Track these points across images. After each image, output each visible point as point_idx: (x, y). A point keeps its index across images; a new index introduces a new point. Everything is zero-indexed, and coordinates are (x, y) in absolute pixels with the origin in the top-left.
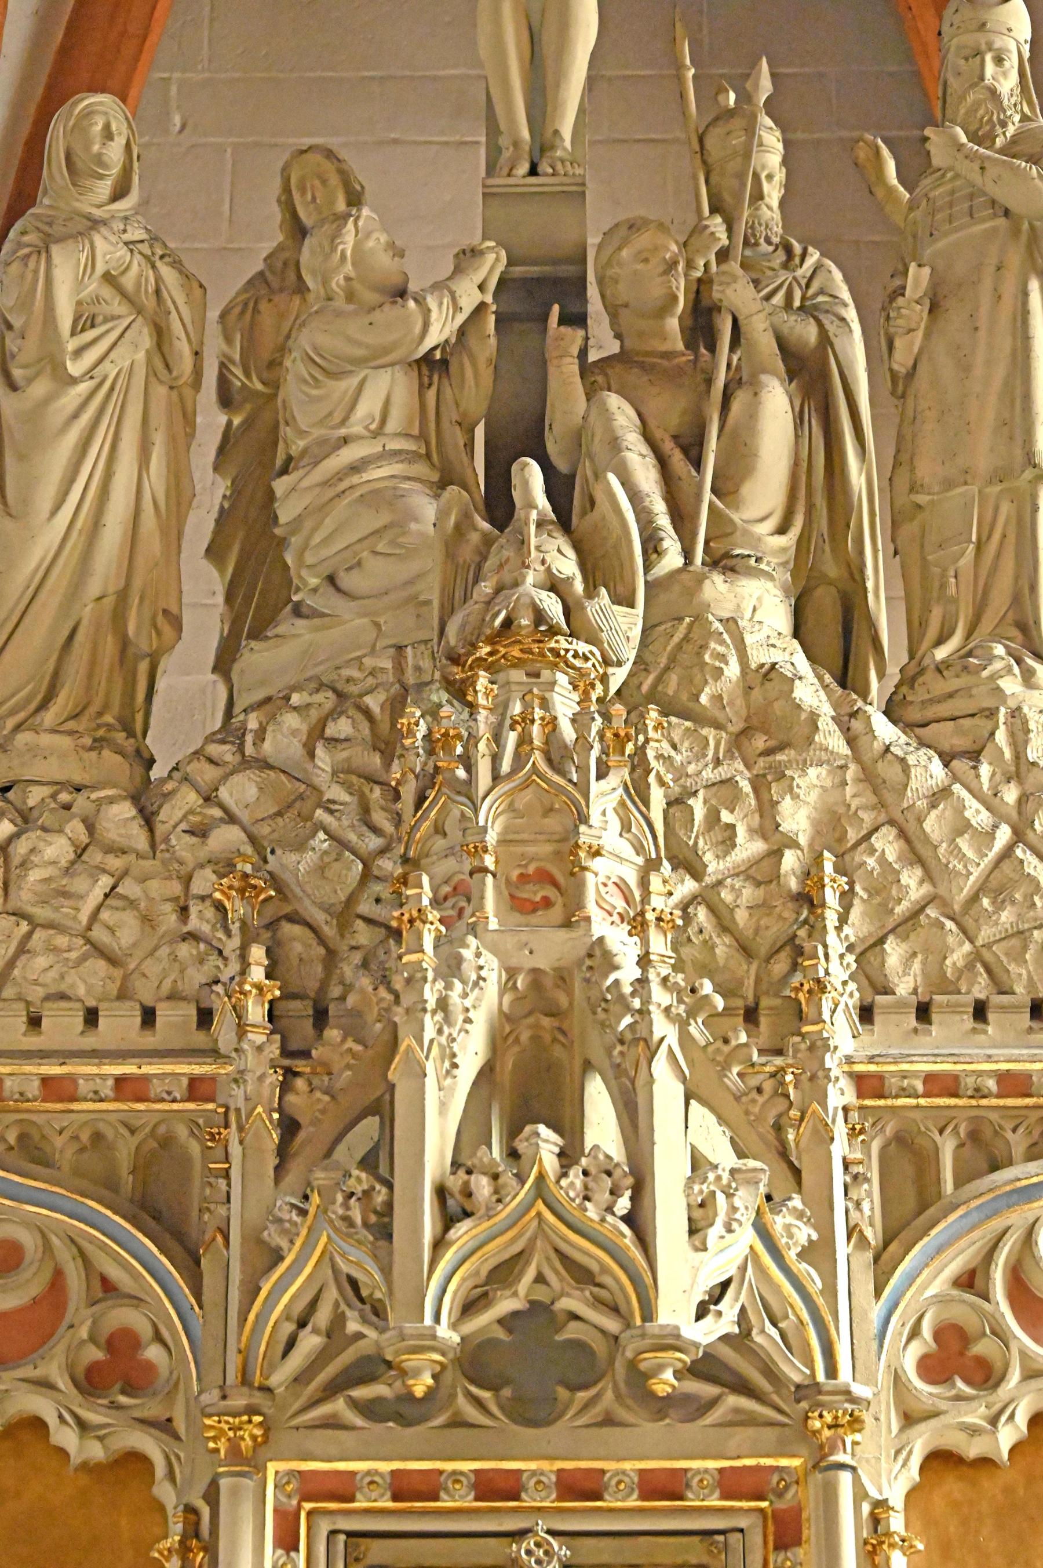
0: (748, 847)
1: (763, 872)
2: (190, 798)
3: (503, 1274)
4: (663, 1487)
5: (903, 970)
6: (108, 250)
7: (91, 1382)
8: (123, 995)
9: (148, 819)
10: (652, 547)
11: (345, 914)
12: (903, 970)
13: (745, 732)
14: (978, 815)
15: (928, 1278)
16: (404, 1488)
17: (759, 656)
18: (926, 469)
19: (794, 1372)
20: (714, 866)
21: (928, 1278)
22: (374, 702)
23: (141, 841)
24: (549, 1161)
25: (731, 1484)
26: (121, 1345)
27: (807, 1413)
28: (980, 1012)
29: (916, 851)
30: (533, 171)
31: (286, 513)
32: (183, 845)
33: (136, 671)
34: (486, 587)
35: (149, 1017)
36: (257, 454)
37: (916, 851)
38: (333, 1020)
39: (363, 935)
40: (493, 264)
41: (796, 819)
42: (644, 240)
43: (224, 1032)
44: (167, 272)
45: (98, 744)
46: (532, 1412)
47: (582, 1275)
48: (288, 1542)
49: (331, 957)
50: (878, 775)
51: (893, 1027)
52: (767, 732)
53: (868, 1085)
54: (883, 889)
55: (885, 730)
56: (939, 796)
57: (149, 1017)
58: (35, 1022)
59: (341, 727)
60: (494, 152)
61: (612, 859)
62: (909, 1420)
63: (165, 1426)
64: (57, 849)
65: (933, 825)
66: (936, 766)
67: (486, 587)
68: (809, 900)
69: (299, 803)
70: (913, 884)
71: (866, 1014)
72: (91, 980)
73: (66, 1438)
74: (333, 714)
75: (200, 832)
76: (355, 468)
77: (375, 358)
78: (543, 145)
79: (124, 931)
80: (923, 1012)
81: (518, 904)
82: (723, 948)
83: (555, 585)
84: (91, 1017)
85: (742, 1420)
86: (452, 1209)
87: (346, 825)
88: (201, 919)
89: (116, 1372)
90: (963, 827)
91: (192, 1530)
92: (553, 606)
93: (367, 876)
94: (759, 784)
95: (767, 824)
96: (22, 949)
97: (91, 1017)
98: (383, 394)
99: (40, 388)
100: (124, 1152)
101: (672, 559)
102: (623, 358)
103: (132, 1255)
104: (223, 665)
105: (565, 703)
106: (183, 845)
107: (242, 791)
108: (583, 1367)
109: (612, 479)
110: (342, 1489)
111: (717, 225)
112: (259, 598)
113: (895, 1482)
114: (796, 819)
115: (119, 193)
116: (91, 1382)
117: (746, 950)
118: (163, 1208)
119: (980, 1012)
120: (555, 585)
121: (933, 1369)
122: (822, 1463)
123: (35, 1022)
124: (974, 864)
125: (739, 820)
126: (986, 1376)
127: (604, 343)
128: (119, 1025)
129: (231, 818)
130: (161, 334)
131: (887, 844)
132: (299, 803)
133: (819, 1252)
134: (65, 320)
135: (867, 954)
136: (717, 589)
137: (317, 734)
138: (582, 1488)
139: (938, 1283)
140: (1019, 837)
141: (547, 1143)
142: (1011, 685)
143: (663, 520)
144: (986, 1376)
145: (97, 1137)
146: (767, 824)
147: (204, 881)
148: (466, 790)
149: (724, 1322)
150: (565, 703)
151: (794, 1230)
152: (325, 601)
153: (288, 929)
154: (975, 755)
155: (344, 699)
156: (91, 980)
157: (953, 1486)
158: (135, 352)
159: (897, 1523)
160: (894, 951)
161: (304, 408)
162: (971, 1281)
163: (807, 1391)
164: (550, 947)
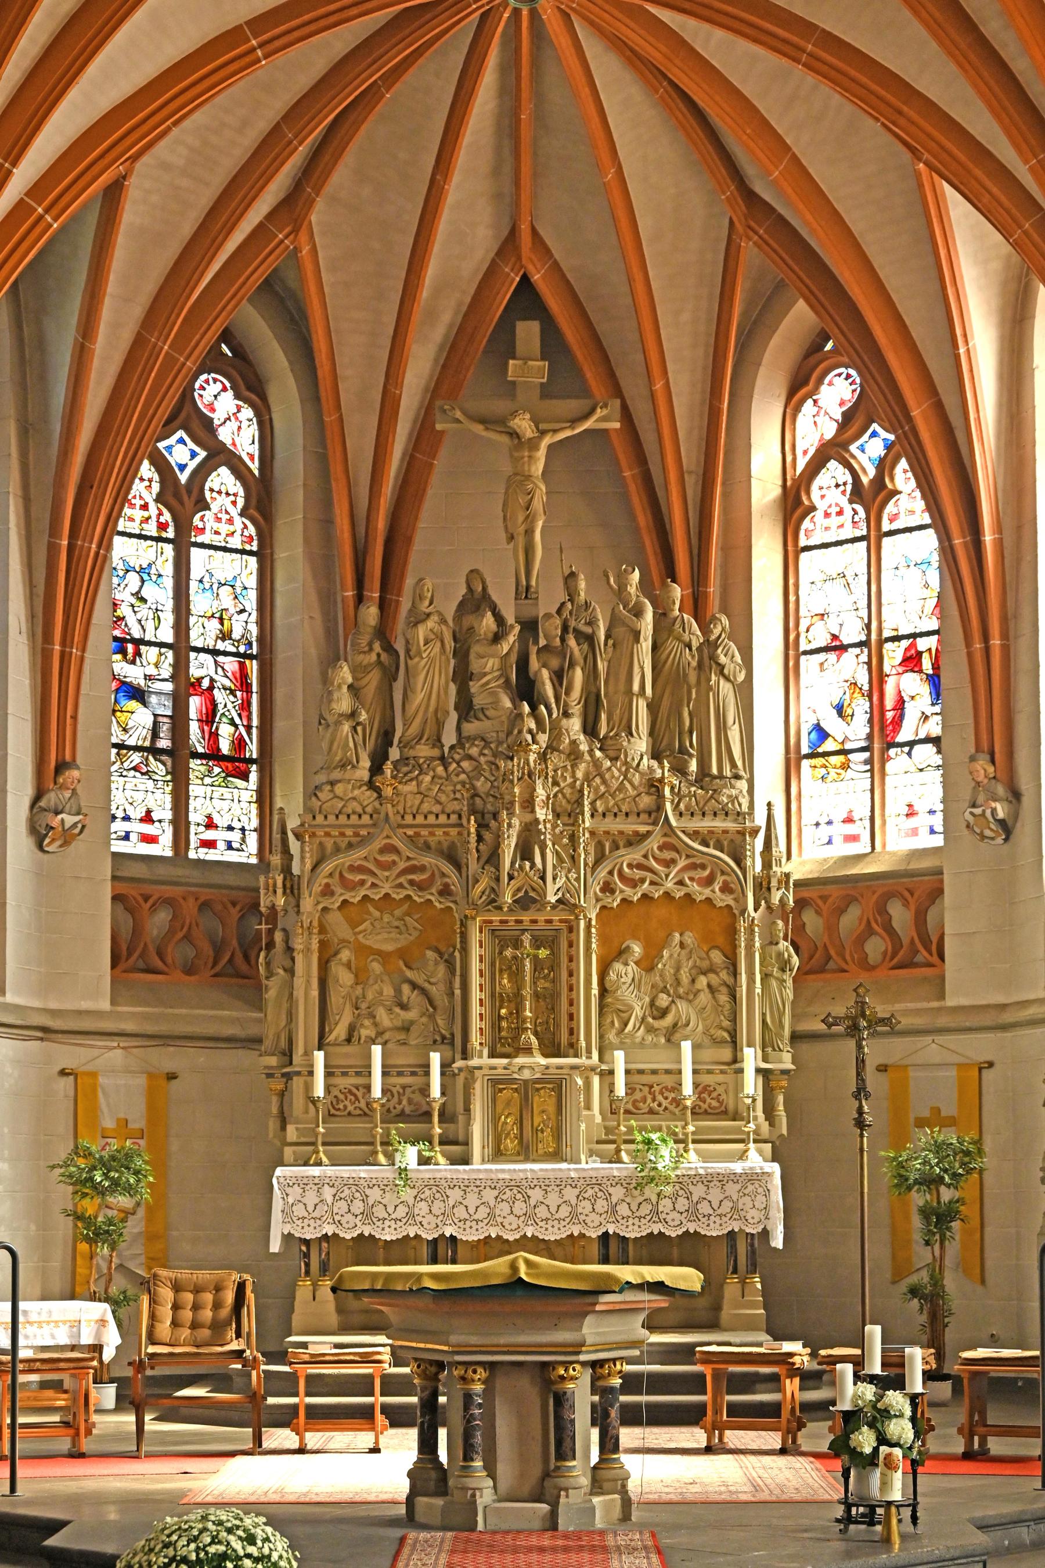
0: (569, 780)
1: (572, 785)
2: (454, 765)
3: (519, 890)
4: (550, 921)
5: (600, 806)
6: (430, 624)
7: (441, 893)
8: (443, 812)
9: (446, 769)
10: (550, 714)
11: (488, 794)
12: (600, 806)
13: (569, 755)
14: (616, 773)
15: (602, 873)
16: (501, 922)
17: (573, 738)
18: (611, 688)
19: (572, 901)
20: (562, 785)
21: (602, 873)
22: (493, 746)
23: (444, 775)
24: (528, 868)
25: (561, 921)
26: (446, 886)
27: (574, 908)
28: (615, 815)
29: (604, 782)
30: (526, 597)
31: (473, 690)
32: (455, 779)
33: (440, 725)
34: (516, 732)
35: (449, 816)
36: (462, 655)
37: (604, 782)
38: (487, 821)
39: (491, 799)
40: (518, 628)
41: (580, 774)
42: (551, 621)
43: (464, 821)
44: (444, 628)
45: (434, 746)
46: (525, 908)
47: (534, 890)
48: (481, 932)
49: (485, 803)
50: (596, 763)
51: (598, 818)
52: (574, 755)
53: (592, 833)
54: (597, 789)
55: (598, 754)
56: (609, 769)
57: (449, 816)
58: (426, 817)
59: (486, 751)
60: (517, 589)
61: (541, 793)
62: (598, 900)
63: (455, 902)
64: (428, 778)
65: (607, 776)
66: (609, 763)
67: (516, 732)
68: (581, 791)
69: (478, 769)
70: (603, 788)
71: (592, 816)
72: (437, 809)
73: (437, 904)
74: (484, 747)
75: (457, 775)
76: (487, 683)
77: (492, 656)
78: (528, 588)
79: (443, 798)
80: (604, 815)
81: (523, 807)
82: (564, 802)
83: (530, 731)
84: (437, 816)
85: (563, 910)
86: (511, 877)
87: (487, 774)
88: (458, 796)
89: (445, 891)
90: (613, 777)
91: (462, 924)
92: (529, 737)
93: (492, 786)
94: (572, 766)
95: (573, 776)
96: (422, 802)
97: (437, 816)
98: (492, 663)
99: (417, 660)
100: (445, 845)
101: (555, 715)
102: (545, 647)
103: (448, 868)
104: (459, 729)
105: (532, 757)
106: (455, 779)
107: (465, 764)
108: (534, 901)
109: (542, 707)
110: (491, 922)
111: (569, 605)
112: (466, 708)
113: (593, 915)
114: (580, 774)
115: (431, 604)
116: (441, 893)
117: (569, 802)
118: (453, 858)
119: (615, 815)
120: (530, 731)
121: (602, 890)
122: (577, 918)
123: (426, 817)
124: (615, 784)
125: (567, 775)
126: (612, 892)
127: (542, 642)
128: (443, 819)
129: (464, 772)
130: (442, 642)
131: (598, 780)
132: (478, 769)
133: (578, 879)
134: (422, 643)
135: (593, 803)
136: (564, 722)
137: (482, 754)
138: (535, 922)
139: (604, 874)
140: (625, 778)
141: (527, 864)
142: (625, 744)
143: (554, 705)
144: (612, 892)
145: (440, 842)
146: (573, 776)
147: (459, 787)
148: (512, 782)
149: (560, 894)
150: (532, 757)
151: (573, 875)
152: (481, 716)
153: (478, 800)
154: (617, 759)
155: (487, 743)
156: (437, 809)
157: (606, 912)
158: (437, 649)
159: (594, 923)
160: (598, 803)
161: (475, 665)
162: (611, 873)
163: (575, 906)
164: (528, 817)
